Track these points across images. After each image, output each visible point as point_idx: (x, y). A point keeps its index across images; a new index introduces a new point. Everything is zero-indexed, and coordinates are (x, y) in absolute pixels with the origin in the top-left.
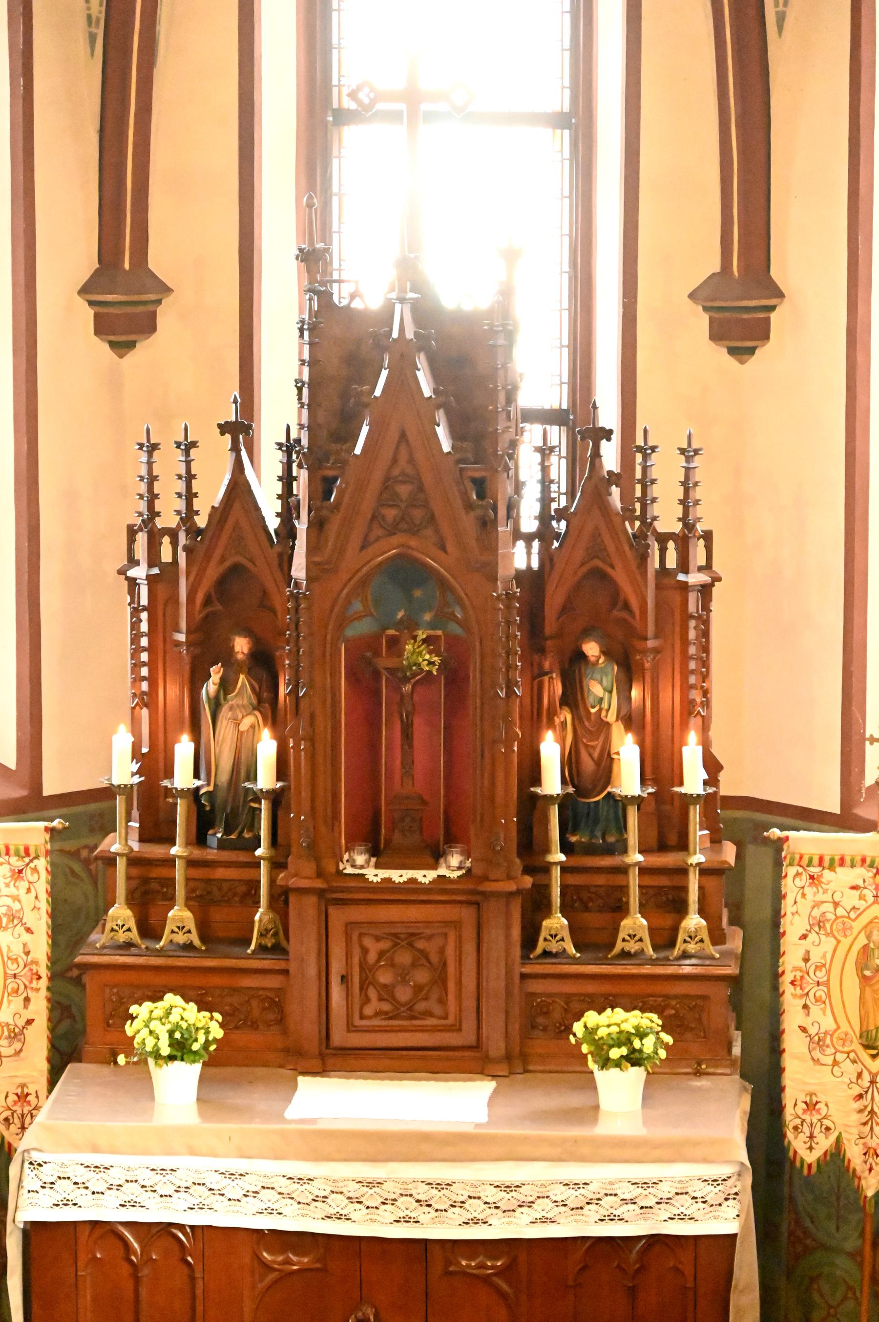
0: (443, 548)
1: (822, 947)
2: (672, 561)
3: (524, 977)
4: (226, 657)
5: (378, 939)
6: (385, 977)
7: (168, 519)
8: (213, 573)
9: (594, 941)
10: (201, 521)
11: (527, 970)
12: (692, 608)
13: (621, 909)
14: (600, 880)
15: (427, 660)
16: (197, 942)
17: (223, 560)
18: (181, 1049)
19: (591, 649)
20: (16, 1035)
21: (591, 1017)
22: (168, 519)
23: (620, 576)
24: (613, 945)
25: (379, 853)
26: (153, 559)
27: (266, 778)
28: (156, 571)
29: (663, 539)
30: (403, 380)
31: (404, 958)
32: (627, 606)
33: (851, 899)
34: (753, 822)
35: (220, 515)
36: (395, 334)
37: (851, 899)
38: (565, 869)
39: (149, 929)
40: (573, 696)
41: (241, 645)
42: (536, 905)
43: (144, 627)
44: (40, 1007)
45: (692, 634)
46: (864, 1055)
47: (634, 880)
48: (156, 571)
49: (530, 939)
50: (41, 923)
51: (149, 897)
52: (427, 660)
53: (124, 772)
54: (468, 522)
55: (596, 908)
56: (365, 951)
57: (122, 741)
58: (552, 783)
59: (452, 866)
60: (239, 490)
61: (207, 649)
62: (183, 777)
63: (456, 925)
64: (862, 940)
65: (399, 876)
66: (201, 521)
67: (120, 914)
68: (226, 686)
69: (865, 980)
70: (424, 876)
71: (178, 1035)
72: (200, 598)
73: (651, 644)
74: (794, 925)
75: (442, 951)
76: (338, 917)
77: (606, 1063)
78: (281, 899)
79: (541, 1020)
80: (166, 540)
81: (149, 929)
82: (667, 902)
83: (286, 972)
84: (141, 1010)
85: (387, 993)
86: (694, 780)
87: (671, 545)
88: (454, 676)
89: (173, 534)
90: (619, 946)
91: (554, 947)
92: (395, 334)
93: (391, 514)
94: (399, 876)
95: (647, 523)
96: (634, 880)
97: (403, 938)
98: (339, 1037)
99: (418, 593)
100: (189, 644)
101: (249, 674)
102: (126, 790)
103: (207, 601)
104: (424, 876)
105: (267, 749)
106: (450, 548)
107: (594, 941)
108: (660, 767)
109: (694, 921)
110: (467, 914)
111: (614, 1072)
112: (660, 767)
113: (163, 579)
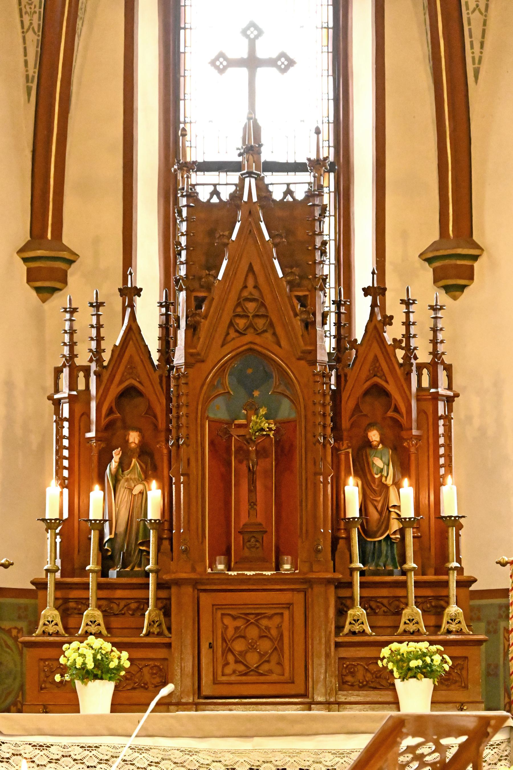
0: (279, 345)
2: (425, 383)
3: (338, 645)
4: (125, 445)
5: (234, 618)
8: (114, 391)
10: (106, 356)
11: (339, 640)
12: (441, 412)
14: (384, 592)
16: (104, 632)
17: (121, 382)
18: (100, 671)
19: (374, 436)
22: (82, 360)
23: (391, 388)
24: (398, 627)
26: (73, 386)
28: (75, 393)
30: (250, 231)
31: (253, 632)
32: (397, 410)
35: (119, 352)
36: (245, 198)
38: (363, 573)
41: (134, 437)
43: (66, 432)
45: (441, 430)
48: (75, 393)
49: (341, 613)
54: (298, 324)
56: (226, 628)
58: (353, 510)
60: (133, 332)
61: (111, 431)
62: (96, 512)
63: (289, 606)
66: (106, 356)
68: (123, 465)
71: (99, 657)
72: (104, 411)
73: (415, 432)
75: (279, 627)
76: (206, 600)
79: (349, 678)
80: (81, 374)
83: (169, 646)
87: (425, 371)
89: (87, 370)
90: (402, 627)
91: (357, 628)
92: (245, 198)
93: (241, 323)
97: (253, 617)
99: (256, 394)
100: (97, 438)
101: (139, 457)
103: (110, 411)
105: (155, 496)
106: (283, 343)
109: (453, 609)
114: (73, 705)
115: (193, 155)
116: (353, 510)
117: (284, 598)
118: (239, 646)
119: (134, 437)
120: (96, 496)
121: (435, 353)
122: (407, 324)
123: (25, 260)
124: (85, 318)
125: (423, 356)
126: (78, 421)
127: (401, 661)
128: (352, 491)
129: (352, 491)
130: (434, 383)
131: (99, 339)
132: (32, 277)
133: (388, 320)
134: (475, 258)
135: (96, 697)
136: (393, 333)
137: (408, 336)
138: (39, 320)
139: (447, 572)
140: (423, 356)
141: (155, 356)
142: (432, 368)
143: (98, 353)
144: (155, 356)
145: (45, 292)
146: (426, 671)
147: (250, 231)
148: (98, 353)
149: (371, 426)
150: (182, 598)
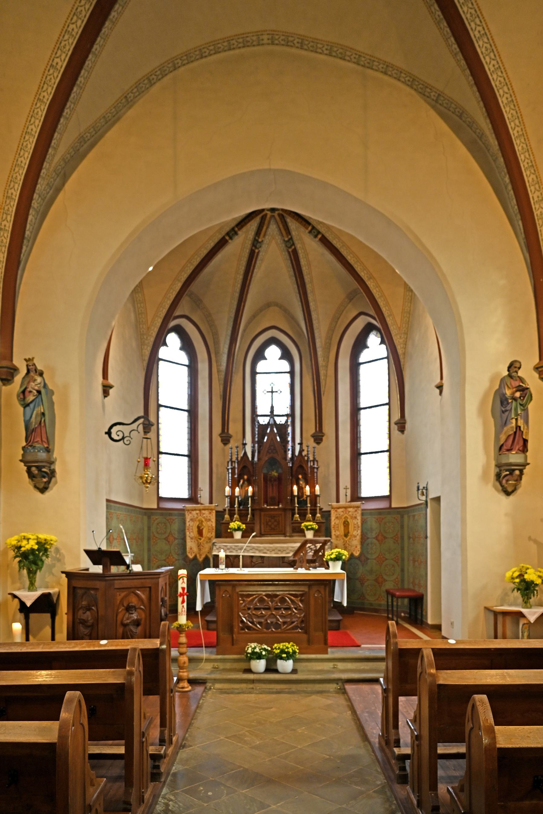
1: (337, 521)
2: (312, 464)
4: (243, 478)
6: (270, 523)
7: (234, 459)
8: (241, 467)
10: (239, 459)
14: (302, 511)
18: (239, 529)
19: (300, 476)
20: (210, 539)
21: (305, 523)
22: (234, 459)
23: (304, 466)
26: (232, 465)
30: (272, 430)
31: (273, 520)
33: (342, 514)
35: (242, 458)
37: (342, 514)
41: (246, 477)
46: (345, 538)
50: (214, 520)
54: (283, 451)
58: (296, 493)
60: (245, 453)
61: (240, 476)
62: (237, 494)
63: (281, 514)
64: (344, 520)
66: (239, 459)
68: (243, 483)
69: (344, 526)
74: (333, 518)
76: (263, 513)
77: (308, 529)
78: (253, 515)
85: (270, 526)
89: (235, 462)
93: (270, 451)
94: (272, 507)
95: (308, 458)
97: (273, 517)
100: (238, 477)
105: (250, 489)
109: (318, 515)
110: (283, 513)
111: (309, 531)
113: (233, 469)
114: (232, 536)
115: (259, 413)
116: (296, 493)
117: (280, 513)
118: (270, 523)
119: (246, 477)
120: (237, 490)
121: (314, 458)
122: (308, 451)
123: (221, 437)
124: (235, 450)
126: (233, 473)
127: (306, 527)
128: (295, 488)
129: (295, 488)
130: (314, 464)
131: (238, 455)
132: (222, 441)
133: (303, 450)
134: (323, 436)
135: (238, 535)
136: (304, 453)
137: (308, 454)
141: (250, 459)
143: (237, 458)
144: (250, 459)
146: (312, 529)
147: (272, 430)
148: (237, 458)
149: (300, 474)
150: (257, 513)
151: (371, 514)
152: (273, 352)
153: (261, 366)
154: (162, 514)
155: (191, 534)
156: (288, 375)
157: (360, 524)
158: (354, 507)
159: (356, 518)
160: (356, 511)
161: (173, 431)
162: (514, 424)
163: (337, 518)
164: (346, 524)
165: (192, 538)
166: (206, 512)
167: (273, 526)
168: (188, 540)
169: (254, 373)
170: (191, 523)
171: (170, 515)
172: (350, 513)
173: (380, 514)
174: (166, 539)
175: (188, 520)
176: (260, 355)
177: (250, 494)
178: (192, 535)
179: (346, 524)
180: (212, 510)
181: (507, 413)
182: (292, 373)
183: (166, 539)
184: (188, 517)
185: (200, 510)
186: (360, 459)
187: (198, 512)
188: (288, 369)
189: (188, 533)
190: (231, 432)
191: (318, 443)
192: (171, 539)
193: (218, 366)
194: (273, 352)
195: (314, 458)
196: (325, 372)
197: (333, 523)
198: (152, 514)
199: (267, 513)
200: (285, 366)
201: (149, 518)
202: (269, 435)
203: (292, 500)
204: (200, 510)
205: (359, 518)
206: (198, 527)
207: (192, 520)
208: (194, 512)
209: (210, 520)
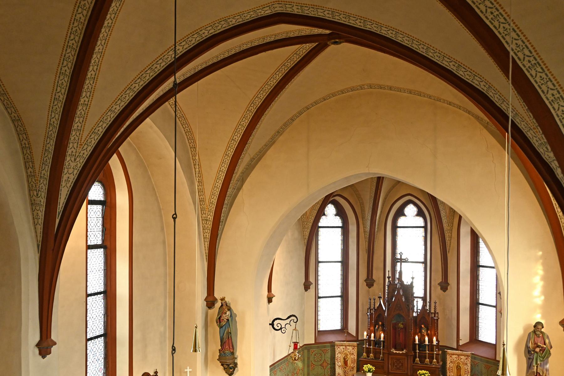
1: (452, 365)
4: (378, 324)
9: (422, 361)
13: (426, 358)
15: (402, 326)
18: (369, 371)
19: (423, 326)
20: (353, 368)
25: (396, 349)
27: (382, 339)
29: (432, 313)
30: (399, 292)
31: (398, 362)
33: (455, 359)
34: (443, 349)
37: (455, 359)
39: (368, 356)
40: (420, 332)
41: (380, 323)
42: (415, 357)
44: (355, 365)
47: (427, 355)
49: (414, 360)
50: (356, 354)
51: (368, 352)
52: (402, 326)
53: (365, 337)
55: (422, 358)
57: (365, 333)
58: (417, 342)
59: (404, 352)
61: (376, 323)
62: (372, 338)
65: (397, 352)
67: (364, 354)
68: (378, 328)
70: (401, 352)
74: (448, 362)
76: (390, 356)
78: (383, 353)
81: (368, 356)
82: (431, 358)
84: (365, 366)
85: (396, 366)
86: (435, 342)
88: (405, 328)
94: (397, 352)
95: (430, 311)
96: (427, 355)
98: (390, 371)
102: (366, 339)
104: (401, 352)
105: (382, 335)
107: (422, 361)
108: (431, 341)
109: (435, 360)
110: (406, 357)
112: (431, 341)
116: (417, 342)
117: (403, 357)
119: (380, 323)
121: (435, 311)
124: (372, 301)
125: (433, 311)
128: (417, 338)
129: (417, 338)
138: (368, 292)
139: (434, 351)
140: (433, 311)
142: (435, 313)
145: (369, 287)
147: (399, 292)
151: (481, 360)
152: (411, 210)
153: (401, 221)
154: (318, 347)
155: (339, 364)
156: (423, 230)
157: (469, 370)
158: (465, 355)
159: (466, 364)
160: (467, 359)
161: (330, 279)
162: (535, 370)
163: (451, 362)
164: (459, 368)
165: (339, 367)
166: (351, 348)
167: (400, 365)
168: (337, 367)
169: (395, 227)
170: (339, 355)
171: (325, 347)
172: (462, 360)
173: (487, 362)
174: (321, 365)
175: (337, 353)
176: (400, 213)
177: (382, 339)
178: (340, 364)
179: (459, 368)
180: (354, 346)
181: (531, 360)
182: (425, 227)
183: (321, 365)
184: (337, 350)
185: (346, 346)
186: (479, 308)
187: (344, 347)
188: (423, 224)
189: (336, 363)
190: (374, 277)
191: (445, 291)
192: (325, 364)
193: (364, 227)
194: (411, 210)
195: (435, 311)
196: (450, 234)
197: (448, 366)
198: (311, 348)
199: (395, 356)
200: (420, 221)
201: (309, 351)
202: (396, 296)
203: (414, 349)
204: (346, 346)
205: (469, 365)
206: (344, 359)
207: (339, 352)
208: (341, 347)
209: (353, 354)
